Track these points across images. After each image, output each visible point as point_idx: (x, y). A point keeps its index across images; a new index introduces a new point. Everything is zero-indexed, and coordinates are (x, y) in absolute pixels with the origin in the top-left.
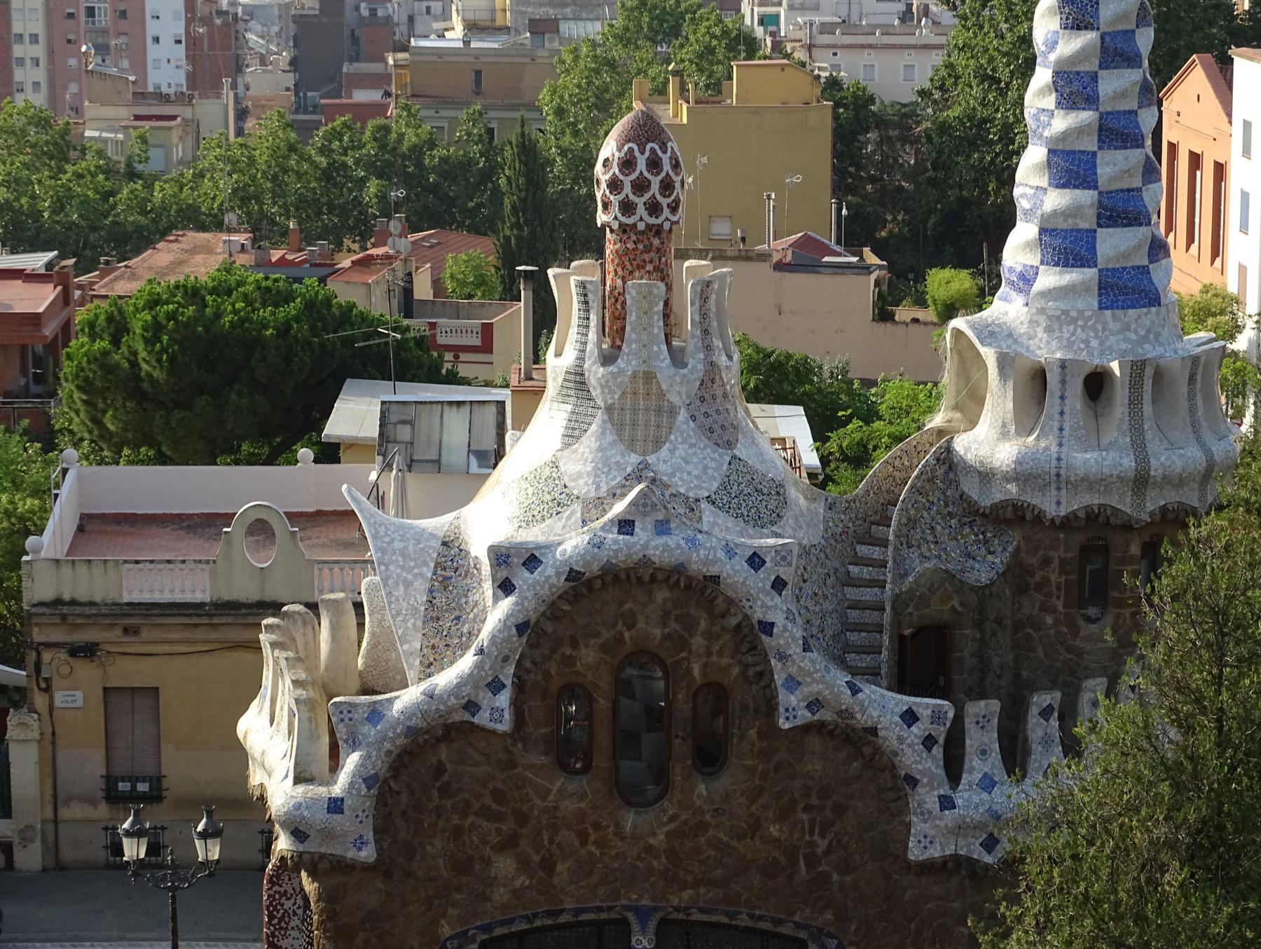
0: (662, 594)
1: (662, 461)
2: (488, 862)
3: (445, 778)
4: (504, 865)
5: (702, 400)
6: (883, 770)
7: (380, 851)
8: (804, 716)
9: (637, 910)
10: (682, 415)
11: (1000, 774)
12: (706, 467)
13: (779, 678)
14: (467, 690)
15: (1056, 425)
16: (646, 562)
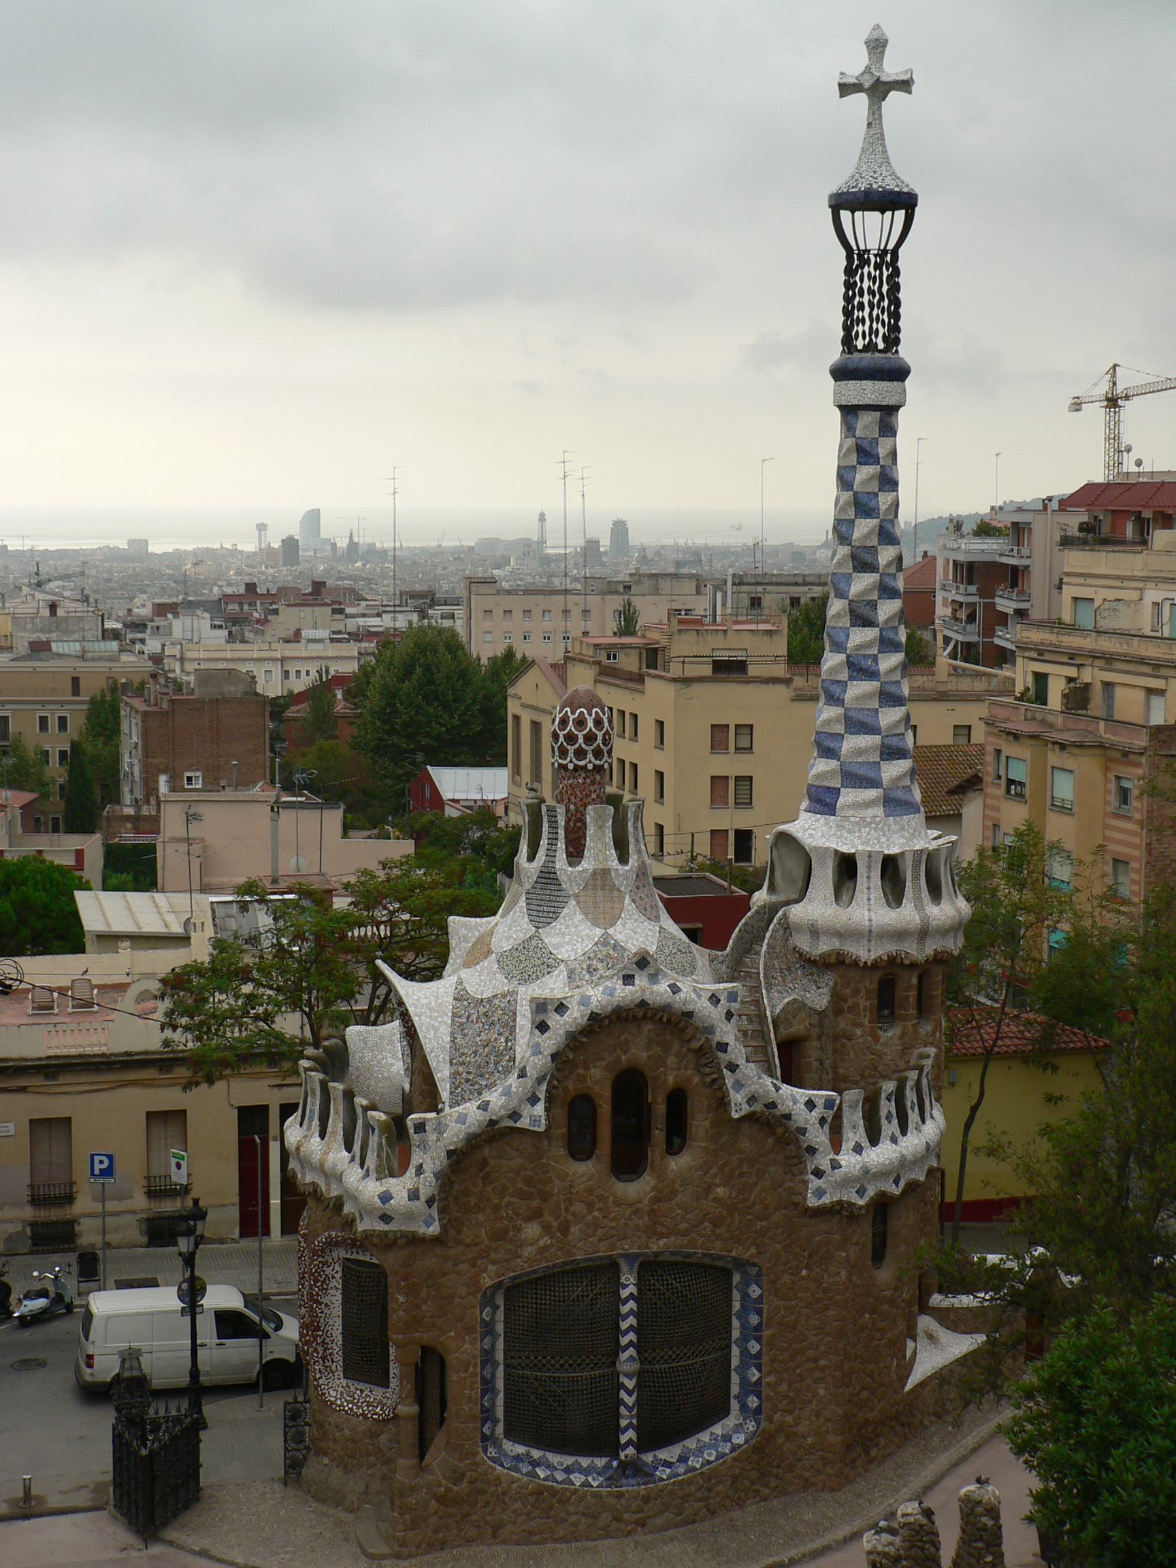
0: (648, 1027)
1: (619, 932)
2: (519, 1230)
3: (488, 1169)
4: (532, 1230)
5: (638, 888)
6: (788, 1144)
7: (443, 1227)
8: (746, 1109)
9: (626, 1257)
10: (627, 900)
11: (865, 1143)
12: (647, 935)
13: (729, 1082)
14: (513, 1104)
15: (865, 897)
16: (643, 1004)
